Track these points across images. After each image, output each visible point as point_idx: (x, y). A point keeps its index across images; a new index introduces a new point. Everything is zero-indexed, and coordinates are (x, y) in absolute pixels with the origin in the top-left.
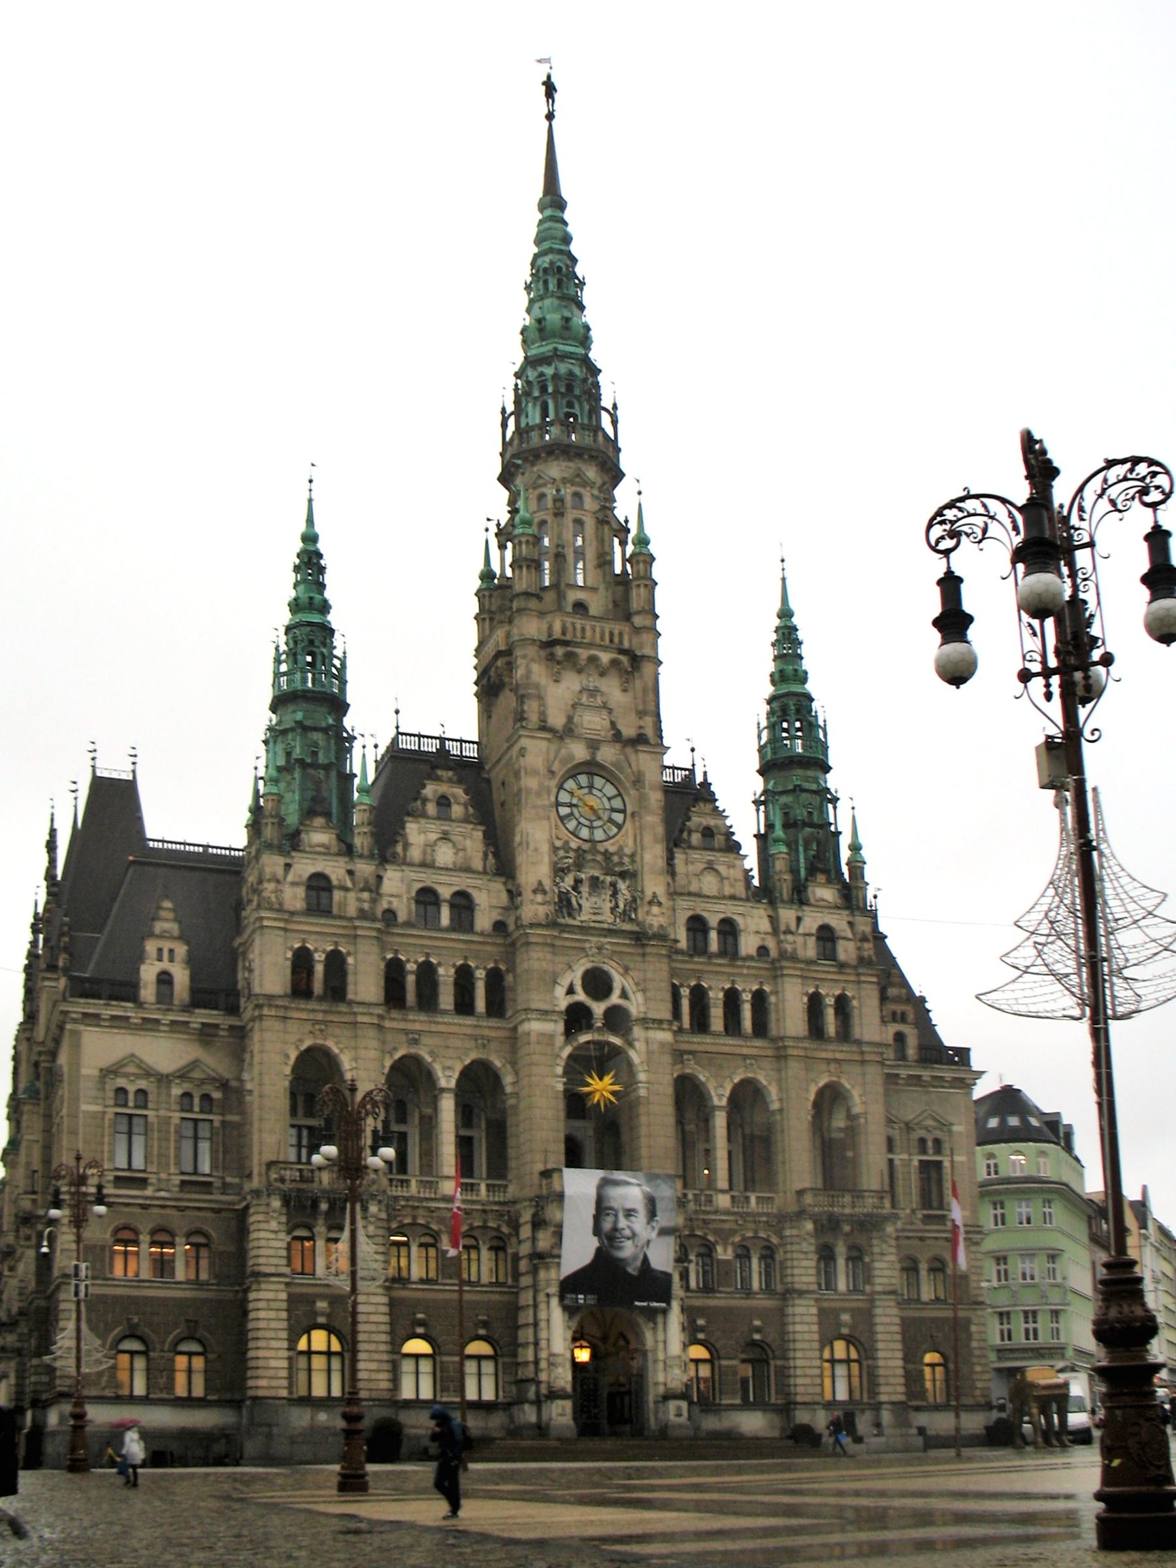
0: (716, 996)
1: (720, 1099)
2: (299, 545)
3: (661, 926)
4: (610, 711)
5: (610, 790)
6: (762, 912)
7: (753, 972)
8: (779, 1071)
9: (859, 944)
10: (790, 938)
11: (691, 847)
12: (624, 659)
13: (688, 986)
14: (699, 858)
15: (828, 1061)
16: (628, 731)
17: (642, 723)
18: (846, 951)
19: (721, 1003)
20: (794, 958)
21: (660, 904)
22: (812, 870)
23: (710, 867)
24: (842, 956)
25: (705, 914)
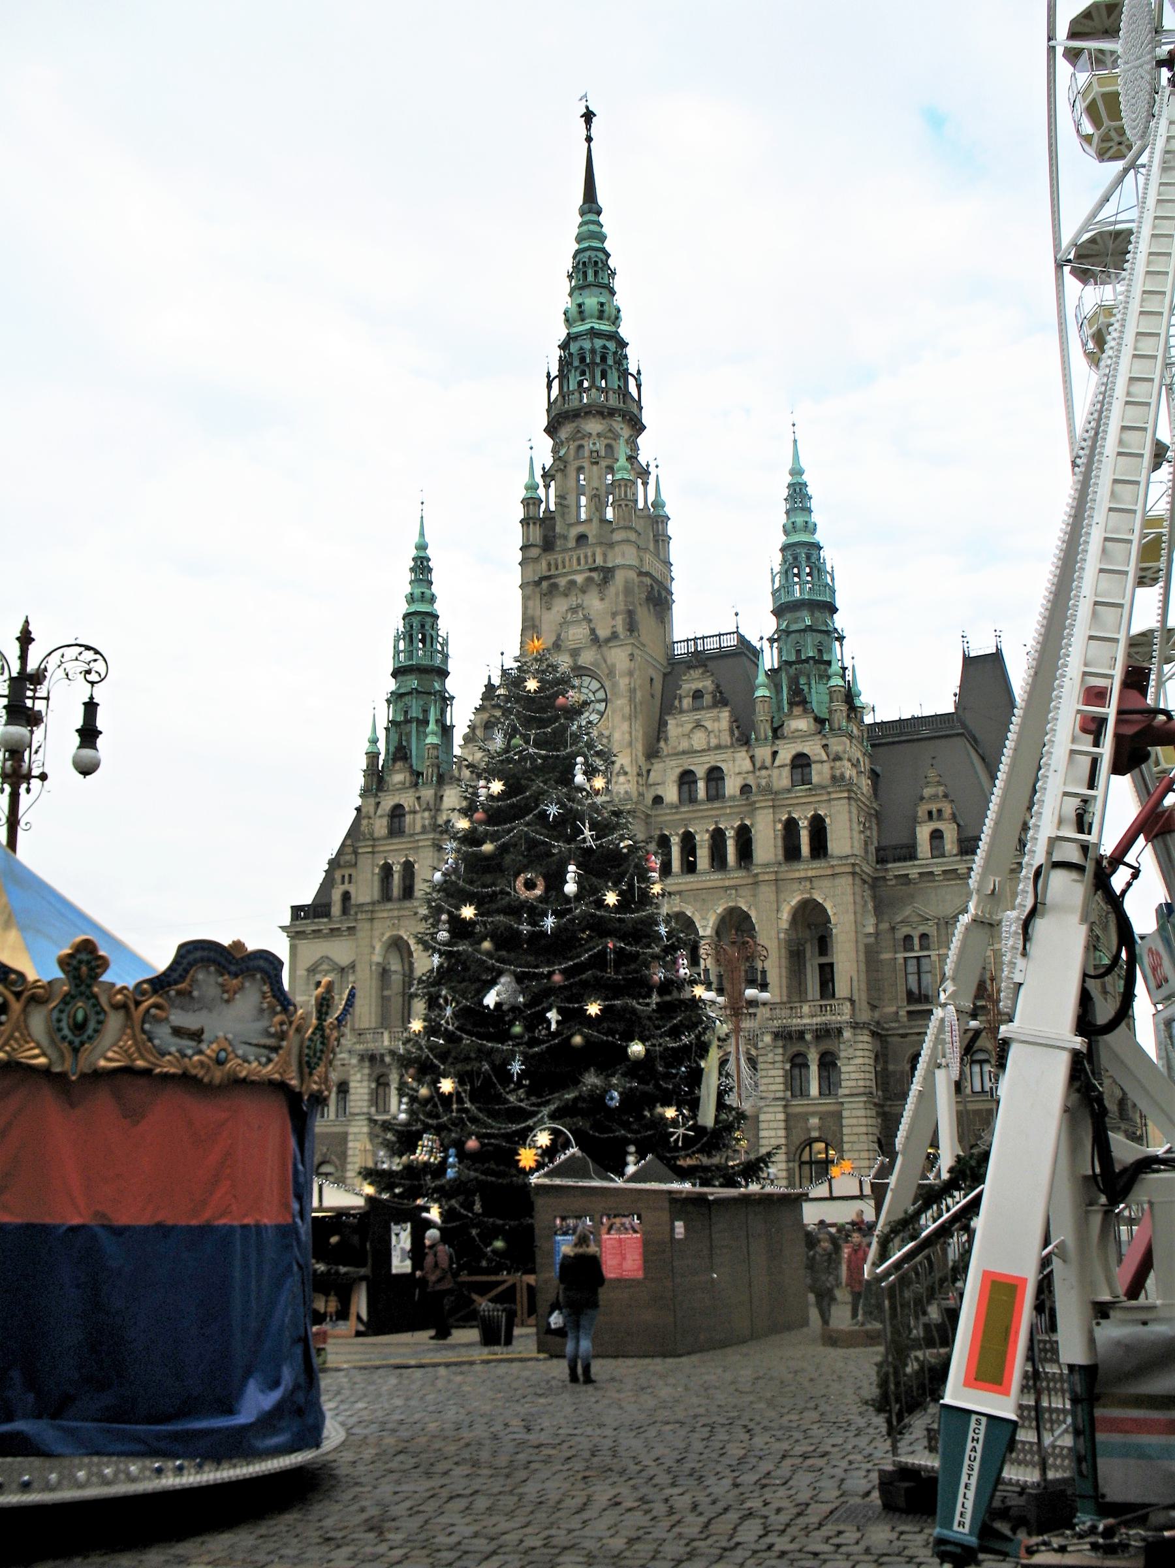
0: (703, 840)
1: (705, 930)
2: (414, 552)
3: (626, 792)
4: (590, 621)
5: (595, 685)
6: (743, 754)
7: (736, 810)
8: (754, 896)
9: (832, 764)
10: (764, 773)
11: (681, 712)
12: (594, 575)
13: (677, 834)
14: (688, 719)
15: (800, 879)
16: (603, 633)
17: (614, 623)
18: (820, 773)
19: (706, 844)
20: (768, 790)
21: (626, 773)
22: (791, 704)
23: (698, 725)
24: (815, 779)
25: (692, 768)
